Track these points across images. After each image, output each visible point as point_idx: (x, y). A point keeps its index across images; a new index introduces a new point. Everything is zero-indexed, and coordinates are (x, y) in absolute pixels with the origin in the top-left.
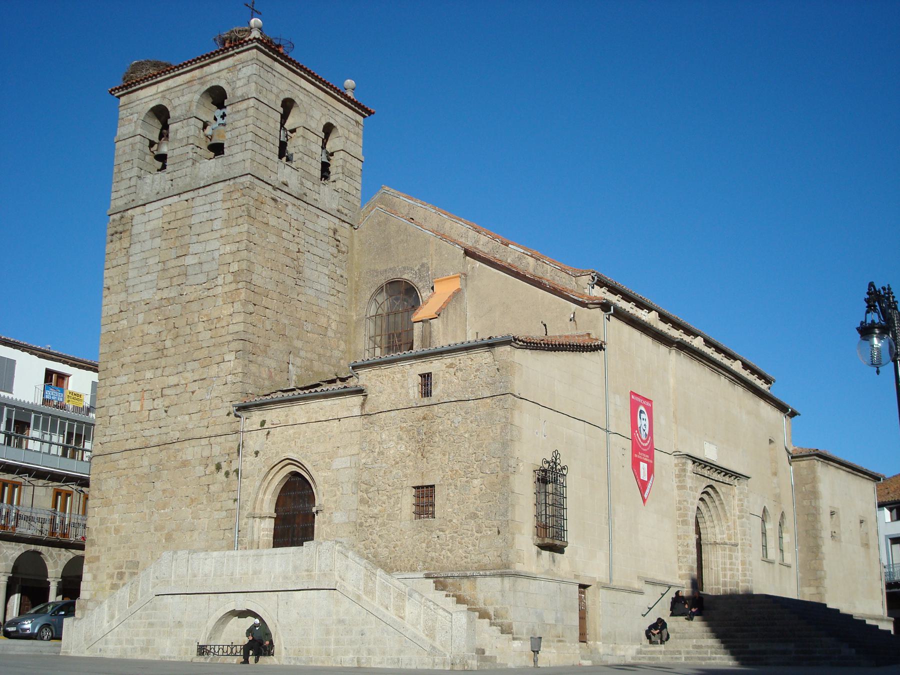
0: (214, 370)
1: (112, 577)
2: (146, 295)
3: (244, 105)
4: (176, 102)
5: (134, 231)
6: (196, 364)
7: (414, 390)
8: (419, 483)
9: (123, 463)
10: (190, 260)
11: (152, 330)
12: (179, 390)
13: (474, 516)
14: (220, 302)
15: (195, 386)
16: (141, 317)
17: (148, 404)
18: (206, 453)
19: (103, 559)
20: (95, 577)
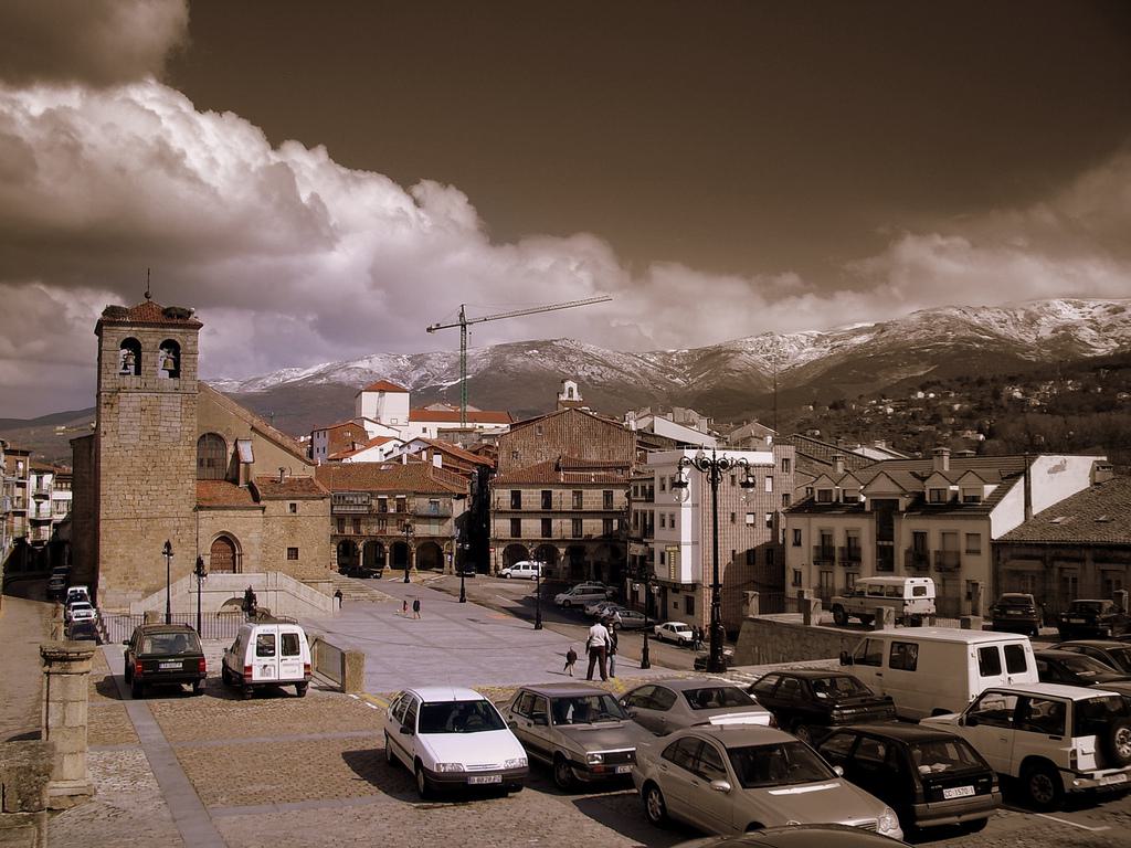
0: (180, 486)
1: (119, 578)
2: (133, 441)
3: (192, 356)
4: (145, 340)
5: (121, 404)
6: (168, 482)
7: (288, 510)
8: (291, 546)
9: (123, 525)
10: (160, 429)
11: (139, 461)
12: (158, 493)
13: (315, 560)
14: (182, 453)
15: (168, 492)
16: (130, 453)
17: (138, 497)
18: (177, 524)
19: (113, 570)
20: (108, 579)
